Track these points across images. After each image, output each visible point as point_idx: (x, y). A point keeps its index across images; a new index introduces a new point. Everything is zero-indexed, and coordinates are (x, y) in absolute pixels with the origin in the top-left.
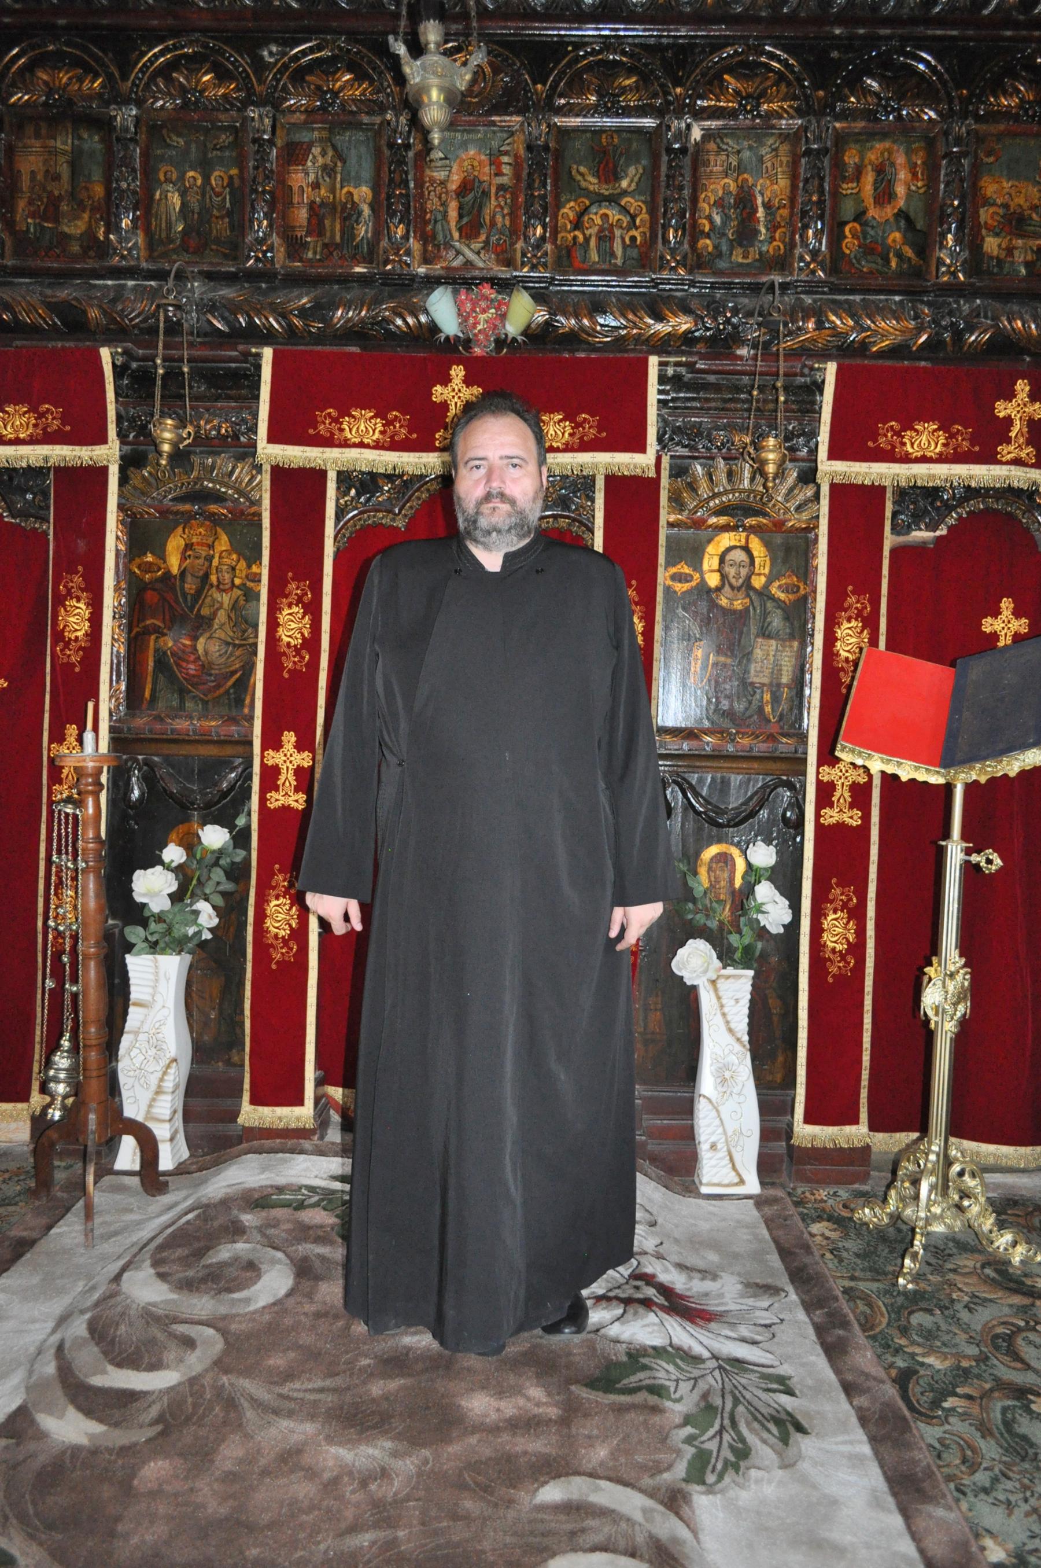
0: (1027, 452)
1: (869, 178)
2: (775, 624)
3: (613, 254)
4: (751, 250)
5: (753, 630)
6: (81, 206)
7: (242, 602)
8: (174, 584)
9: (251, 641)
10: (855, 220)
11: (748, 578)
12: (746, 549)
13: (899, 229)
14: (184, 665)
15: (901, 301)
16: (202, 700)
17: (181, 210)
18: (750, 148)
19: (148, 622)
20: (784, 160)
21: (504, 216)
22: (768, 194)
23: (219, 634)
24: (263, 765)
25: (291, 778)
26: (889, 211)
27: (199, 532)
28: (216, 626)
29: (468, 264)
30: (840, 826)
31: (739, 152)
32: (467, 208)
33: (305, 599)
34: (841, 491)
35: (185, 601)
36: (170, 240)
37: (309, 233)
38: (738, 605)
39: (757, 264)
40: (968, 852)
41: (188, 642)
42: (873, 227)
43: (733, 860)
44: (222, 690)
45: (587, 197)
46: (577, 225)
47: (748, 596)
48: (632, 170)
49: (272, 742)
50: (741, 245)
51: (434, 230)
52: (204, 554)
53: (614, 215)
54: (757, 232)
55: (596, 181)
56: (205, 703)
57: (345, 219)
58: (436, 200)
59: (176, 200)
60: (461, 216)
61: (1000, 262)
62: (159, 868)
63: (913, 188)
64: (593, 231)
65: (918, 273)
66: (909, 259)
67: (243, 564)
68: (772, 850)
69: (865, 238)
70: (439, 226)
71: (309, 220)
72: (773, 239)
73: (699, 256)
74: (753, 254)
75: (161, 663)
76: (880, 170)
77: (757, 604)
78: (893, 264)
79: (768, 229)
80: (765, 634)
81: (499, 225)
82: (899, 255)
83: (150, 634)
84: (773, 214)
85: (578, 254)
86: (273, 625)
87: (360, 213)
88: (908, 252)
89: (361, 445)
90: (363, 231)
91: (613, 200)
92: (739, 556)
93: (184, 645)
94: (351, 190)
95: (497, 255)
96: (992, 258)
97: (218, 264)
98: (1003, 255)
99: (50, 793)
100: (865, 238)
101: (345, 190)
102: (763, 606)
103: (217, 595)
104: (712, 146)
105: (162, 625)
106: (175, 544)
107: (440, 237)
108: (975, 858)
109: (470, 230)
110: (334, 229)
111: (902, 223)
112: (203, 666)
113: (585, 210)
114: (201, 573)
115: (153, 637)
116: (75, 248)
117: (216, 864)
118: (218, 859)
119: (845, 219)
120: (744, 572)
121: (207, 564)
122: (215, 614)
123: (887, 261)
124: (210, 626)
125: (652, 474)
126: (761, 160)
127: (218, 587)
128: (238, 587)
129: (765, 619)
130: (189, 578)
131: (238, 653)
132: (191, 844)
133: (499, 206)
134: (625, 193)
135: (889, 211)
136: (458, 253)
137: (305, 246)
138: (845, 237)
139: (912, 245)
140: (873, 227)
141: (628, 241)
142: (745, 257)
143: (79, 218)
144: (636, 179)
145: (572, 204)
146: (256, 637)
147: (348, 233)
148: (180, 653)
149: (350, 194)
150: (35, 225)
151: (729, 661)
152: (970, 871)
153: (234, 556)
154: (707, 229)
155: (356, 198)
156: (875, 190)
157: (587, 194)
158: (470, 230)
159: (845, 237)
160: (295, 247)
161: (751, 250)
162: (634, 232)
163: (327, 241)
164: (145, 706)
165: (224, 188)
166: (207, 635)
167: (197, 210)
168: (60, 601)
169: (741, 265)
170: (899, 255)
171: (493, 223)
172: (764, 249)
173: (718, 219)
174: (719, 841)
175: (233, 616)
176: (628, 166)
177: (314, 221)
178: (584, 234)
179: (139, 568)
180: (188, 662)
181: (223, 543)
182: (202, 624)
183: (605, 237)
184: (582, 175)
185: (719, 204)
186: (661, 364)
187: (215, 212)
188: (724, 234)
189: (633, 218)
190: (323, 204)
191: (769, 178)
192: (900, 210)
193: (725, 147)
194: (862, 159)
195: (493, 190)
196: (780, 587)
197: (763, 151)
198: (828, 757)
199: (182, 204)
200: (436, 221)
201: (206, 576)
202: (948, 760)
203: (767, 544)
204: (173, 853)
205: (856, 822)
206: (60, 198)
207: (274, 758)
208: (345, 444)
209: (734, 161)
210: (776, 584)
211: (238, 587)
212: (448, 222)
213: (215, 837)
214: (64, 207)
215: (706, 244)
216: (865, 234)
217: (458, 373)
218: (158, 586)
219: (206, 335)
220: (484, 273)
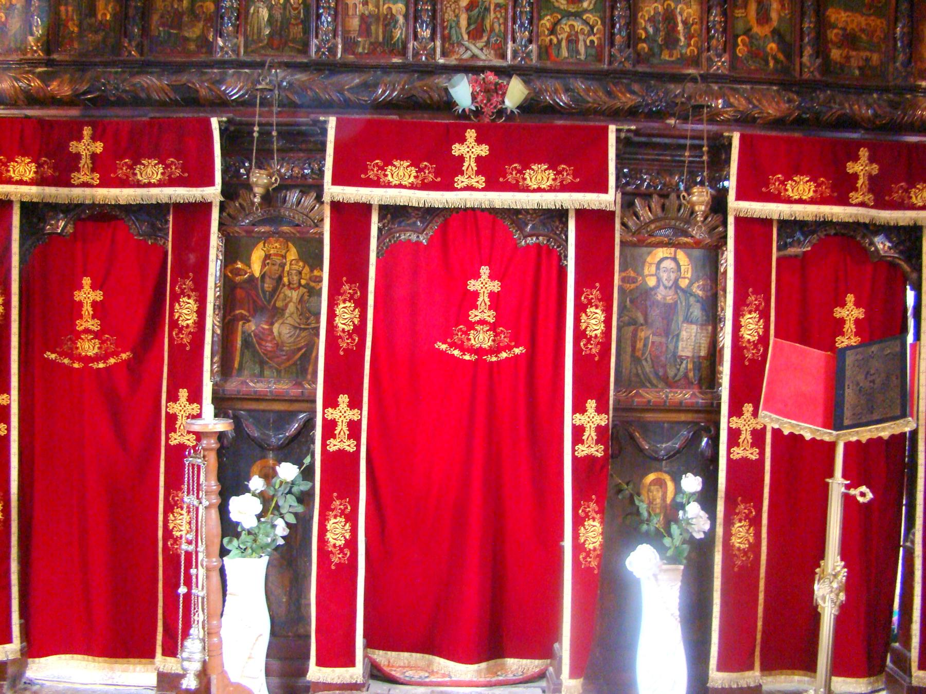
0: (869, 198)
2: (695, 313)
3: (578, 52)
4: (675, 52)
5: (681, 319)
6: (197, 18)
7: (306, 297)
8: (257, 285)
9: (313, 325)
11: (676, 281)
12: (675, 259)
13: (774, 42)
14: (264, 343)
15: (778, 91)
16: (276, 369)
17: (269, 20)
19: (237, 312)
21: (500, 25)
22: (685, 15)
23: (290, 321)
24: (324, 419)
25: (345, 429)
27: (275, 246)
28: (287, 315)
29: (474, 56)
30: (745, 460)
32: (472, 21)
33: (356, 297)
34: (743, 222)
35: (265, 297)
36: (261, 41)
37: (360, 35)
38: (669, 300)
40: (848, 487)
41: (266, 327)
42: (757, 40)
43: (666, 484)
44: (291, 362)
45: (560, 14)
46: (553, 31)
47: (676, 293)
49: (331, 402)
50: (667, 48)
51: (450, 33)
52: (278, 262)
53: (578, 25)
54: (677, 40)
56: (279, 372)
57: (385, 26)
58: (451, 13)
59: (264, 13)
60: (469, 25)
61: (842, 67)
62: (248, 495)
63: (783, 15)
64: (564, 36)
66: (782, 62)
67: (307, 269)
68: (699, 480)
69: (751, 47)
70: (453, 31)
71: (360, 26)
72: (689, 45)
73: (638, 55)
74: (676, 54)
75: (247, 343)
77: (683, 299)
78: (771, 64)
79: (685, 38)
80: (688, 320)
81: (497, 31)
83: (239, 320)
84: (689, 29)
85: (554, 52)
86: (331, 315)
87: (397, 22)
88: (781, 57)
89: (400, 186)
90: (398, 34)
91: (577, 15)
92: (669, 264)
93: (263, 329)
94: (391, 6)
95: (495, 51)
96: (836, 63)
97: (294, 57)
98: (843, 61)
99: (167, 438)
100: (751, 47)
101: (386, 6)
102: (687, 300)
103: (288, 292)
105: (247, 314)
106: (257, 256)
107: (454, 38)
108: (852, 492)
109: (476, 33)
110: (378, 32)
111: (776, 38)
112: (277, 345)
113: (558, 22)
114: (277, 275)
115: (241, 323)
116: (192, 47)
117: (290, 492)
118: (291, 488)
119: (739, 32)
120: (673, 276)
121: (281, 269)
122: (286, 306)
123: (767, 63)
124: (283, 315)
125: (612, 209)
127: (289, 285)
128: (304, 286)
129: (688, 310)
130: (267, 280)
131: (303, 334)
132: (269, 475)
133: (496, 17)
134: (586, 11)
136: (467, 49)
137: (356, 44)
139: (783, 52)
141: (588, 43)
142: (671, 55)
143: (194, 26)
145: (548, 17)
146: (318, 321)
147: (389, 36)
148: (261, 335)
149: (390, 9)
150: (164, 31)
151: (663, 340)
152: (848, 501)
153: (301, 264)
154: (643, 37)
155: (394, 11)
156: (758, 14)
157: (558, 10)
158: (476, 33)
159: (738, 45)
160: (349, 45)
161: (675, 52)
162: (592, 38)
163: (373, 40)
164: (235, 372)
165: (300, 5)
166: (280, 321)
167: (280, 19)
168: (175, 298)
169: (668, 62)
170: (775, 58)
171: (492, 30)
172: (684, 51)
173: (651, 30)
174: (656, 470)
175: (299, 307)
177: (364, 26)
178: (558, 38)
179: (231, 272)
180: (266, 341)
181: (293, 254)
182: (276, 313)
183: (572, 41)
185: (652, 20)
186: (618, 131)
187: (293, 21)
188: (655, 41)
189: (592, 28)
190: (370, 15)
195: (492, 7)
196: (698, 287)
198: (736, 411)
199: (269, 15)
200: (451, 28)
201: (280, 278)
202: (833, 421)
203: (689, 256)
204: (256, 483)
205: (754, 457)
206: (183, 14)
207: (331, 414)
208: (388, 185)
210: (696, 285)
211: (304, 286)
212: (460, 28)
213: (288, 471)
214: (186, 19)
216: (751, 43)
217: (471, 134)
218: (247, 286)
219: (284, 106)
220: (487, 63)
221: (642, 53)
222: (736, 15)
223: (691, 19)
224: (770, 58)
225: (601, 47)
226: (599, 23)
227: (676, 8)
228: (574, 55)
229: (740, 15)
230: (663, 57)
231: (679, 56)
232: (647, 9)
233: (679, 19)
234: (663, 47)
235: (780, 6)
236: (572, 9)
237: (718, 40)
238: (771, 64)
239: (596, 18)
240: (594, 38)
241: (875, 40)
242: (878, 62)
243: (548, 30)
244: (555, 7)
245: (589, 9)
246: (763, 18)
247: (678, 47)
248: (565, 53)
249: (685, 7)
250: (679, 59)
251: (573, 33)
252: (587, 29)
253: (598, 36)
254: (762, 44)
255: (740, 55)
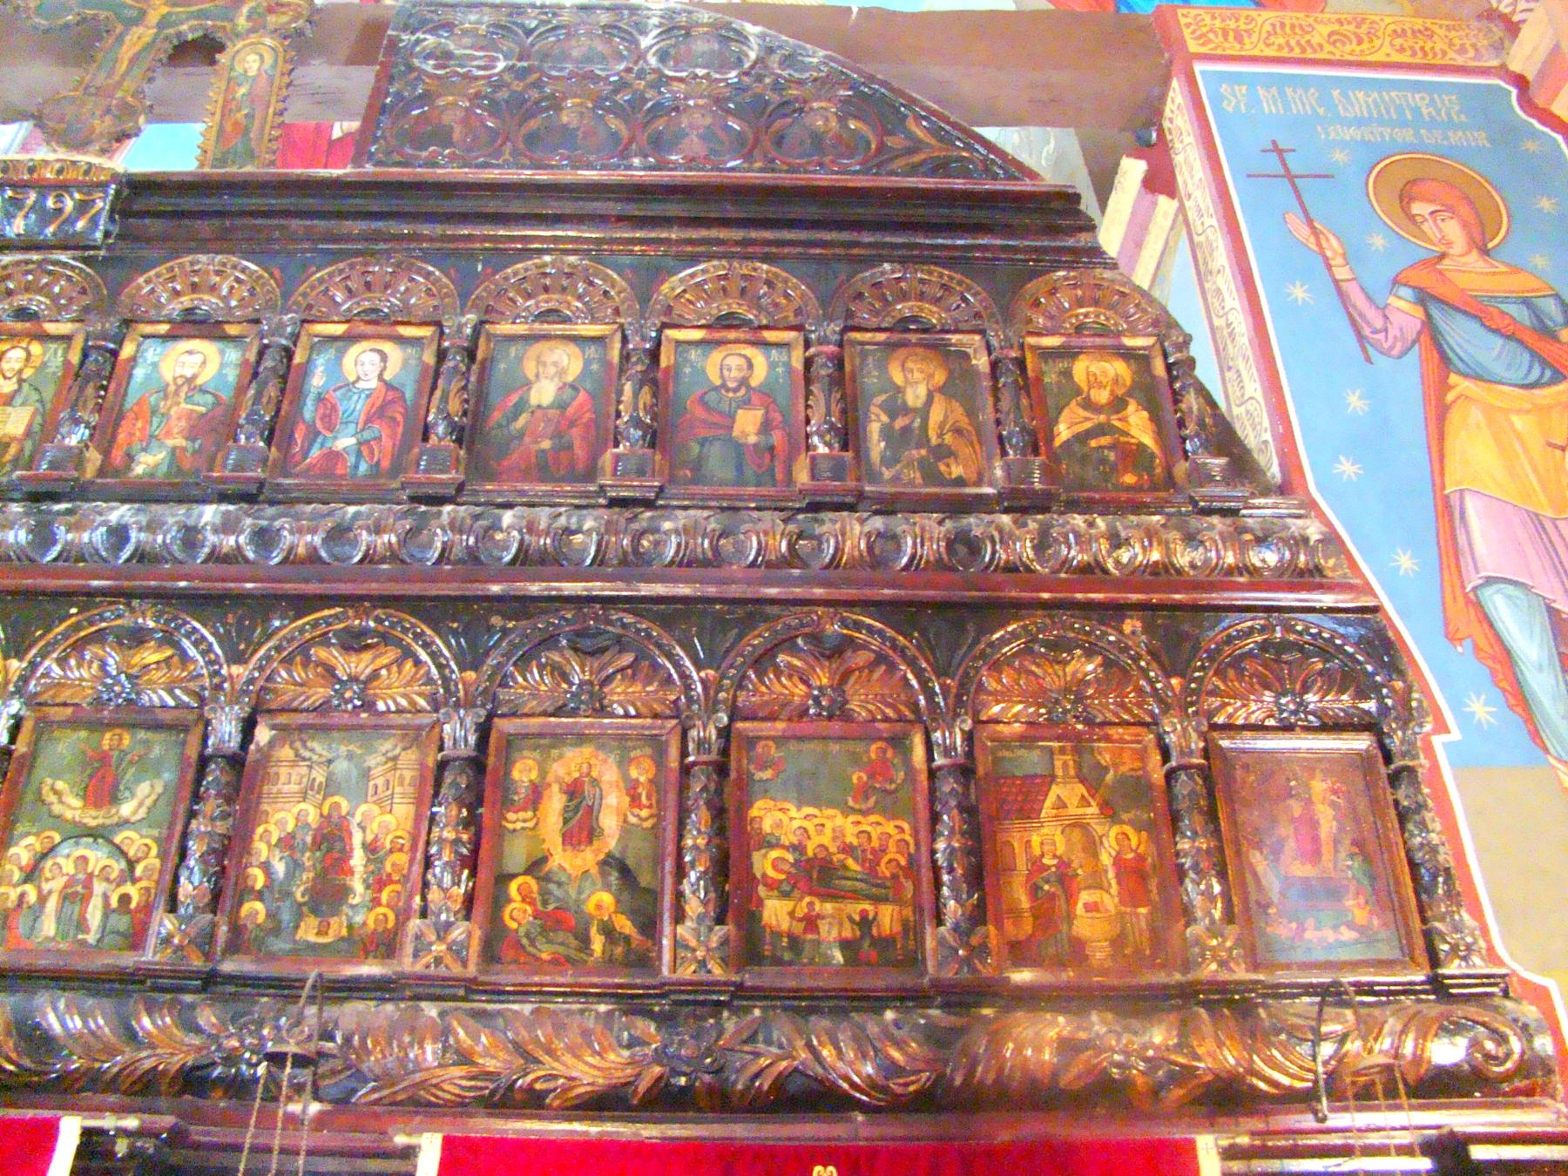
1: (555, 803)
4: (334, 921)
10: (528, 871)
13: (607, 887)
15: (609, 1013)
18: (350, 757)
20: (408, 775)
26: (588, 858)
31: (330, 762)
39: (343, 946)
42: (560, 884)
46: (32, 874)
48: (143, 789)
50: (315, 911)
53: (98, 857)
54: (345, 891)
55: (77, 803)
61: (795, 942)
63: (633, 820)
64: (57, 884)
65: (644, 961)
66: (627, 939)
69: (545, 903)
72: (376, 902)
74: (338, 927)
76: (573, 791)
78: (598, 943)
79: (368, 887)
82: (609, 932)
85: (22, 923)
88: (625, 925)
91: (95, 834)
96: (777, 934)
98: (798, 928)
100: (545, 903)
104: (286, 753)
111: (614, 877)
113: (51, 851)
123: (585, 941)
126: (366, 774)
134: (125, 823)
135: (588, 858)
138: (510, 900)
139: (633, 914)
140: (560, 884)
141: (114, 903)
144: (149, 802)
145: (31, 840)
154: (259, 885)
156: (566, 821)
159: (510, 900)
170: (609, 932)
172: (358, 919)
173: (280, 868)
176: (138, 781)
183: (75, 895)
184: (56, 792)
185: (287, 842)
188: (289, 894)
189: (131, 864)
191: (378, 802)
192: (609, 855)
193: (307, 754)
194: (543, 773)
197: (371, 761)
209: (319, 776)
215: (254, 910)
216: (545, 893)
221: (250, 926)
222: (510, 826)
223: (390, 837)
224: (593, 931)
225: (147, 909)
226: (154, 851)
227: (351, 814)
228: (72, 933)
229: (519, 825)
230: (300, 935)
231: (344, 932)
232: (278, 816)
233: (357, 839)
234: (305, 909)
235: (628, 799)
236: (92, 819)
237: (448, 886)
238: (598, 943)
239: (148, 841)
240: (133, 891)
241: (884, 870)
242: (898, 928)
243: (21, 869)
244: (50, 814)
245: (133, 819)
246: (580, 829)
247: (345, 909)
248: (48, 926)
249: (376, 810)
250: (342, 939)
251: (81, 876)
252: (118, 866)
253: (144, 883)
254: (573, 893)
255: (514, 925)
